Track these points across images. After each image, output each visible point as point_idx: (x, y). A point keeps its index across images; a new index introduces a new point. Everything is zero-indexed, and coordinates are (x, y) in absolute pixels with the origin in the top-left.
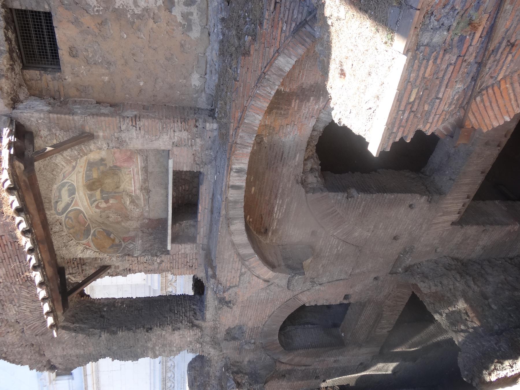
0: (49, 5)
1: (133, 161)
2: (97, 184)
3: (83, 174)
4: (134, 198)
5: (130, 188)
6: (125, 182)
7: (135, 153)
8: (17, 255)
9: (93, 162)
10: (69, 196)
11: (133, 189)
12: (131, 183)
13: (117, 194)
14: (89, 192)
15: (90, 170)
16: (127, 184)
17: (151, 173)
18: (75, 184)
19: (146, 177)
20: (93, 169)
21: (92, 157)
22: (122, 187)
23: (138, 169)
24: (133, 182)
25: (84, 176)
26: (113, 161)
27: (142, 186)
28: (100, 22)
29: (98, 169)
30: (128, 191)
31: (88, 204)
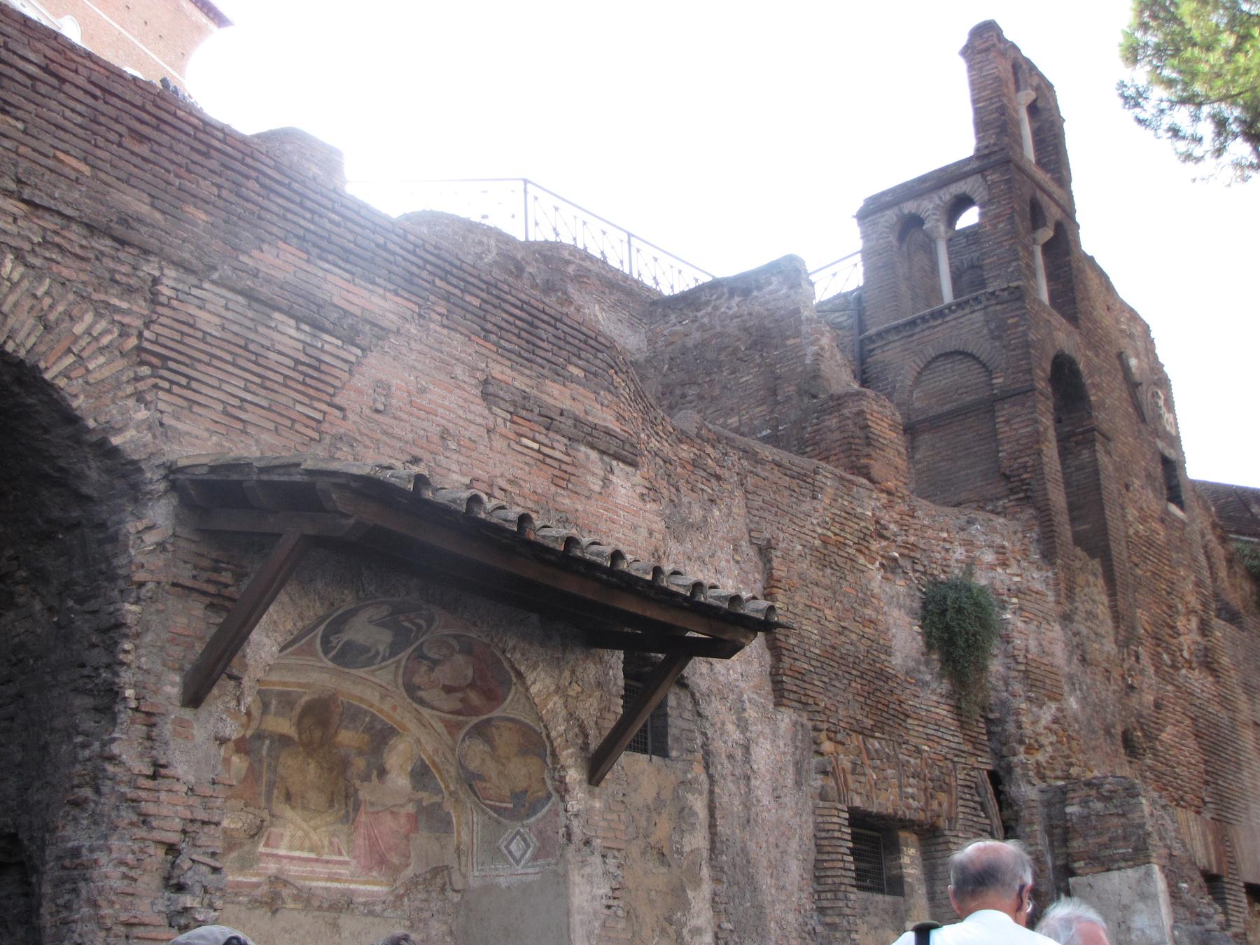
0: (676, 759)
1: (371, 869)
2: (318, 734)
3: (372, 706)
4: (247, 848)
5: (286, 841)
6: (305, 826)
7: (395, 881)
8: (269, 409)
9: (386, 743)
10: (348, 645)
11: (282, 852)
12: (302, 849)
13: (263, 788)
14: (306, 698)
15: (369, 729)
16: (300, 833)
17: (335, 926)
18: (361, 672)
19: (316, 903)
20: (367, 737)
21: (401, 746)
22: (288, 813)
23: (346, 881)
24: (305, 855)
25: (365, 707)
26: (372, 804)
27: (286, 883)
28: (665, 851)
29: (360, 753)
30: (273, 829)
31: (271, 682)
